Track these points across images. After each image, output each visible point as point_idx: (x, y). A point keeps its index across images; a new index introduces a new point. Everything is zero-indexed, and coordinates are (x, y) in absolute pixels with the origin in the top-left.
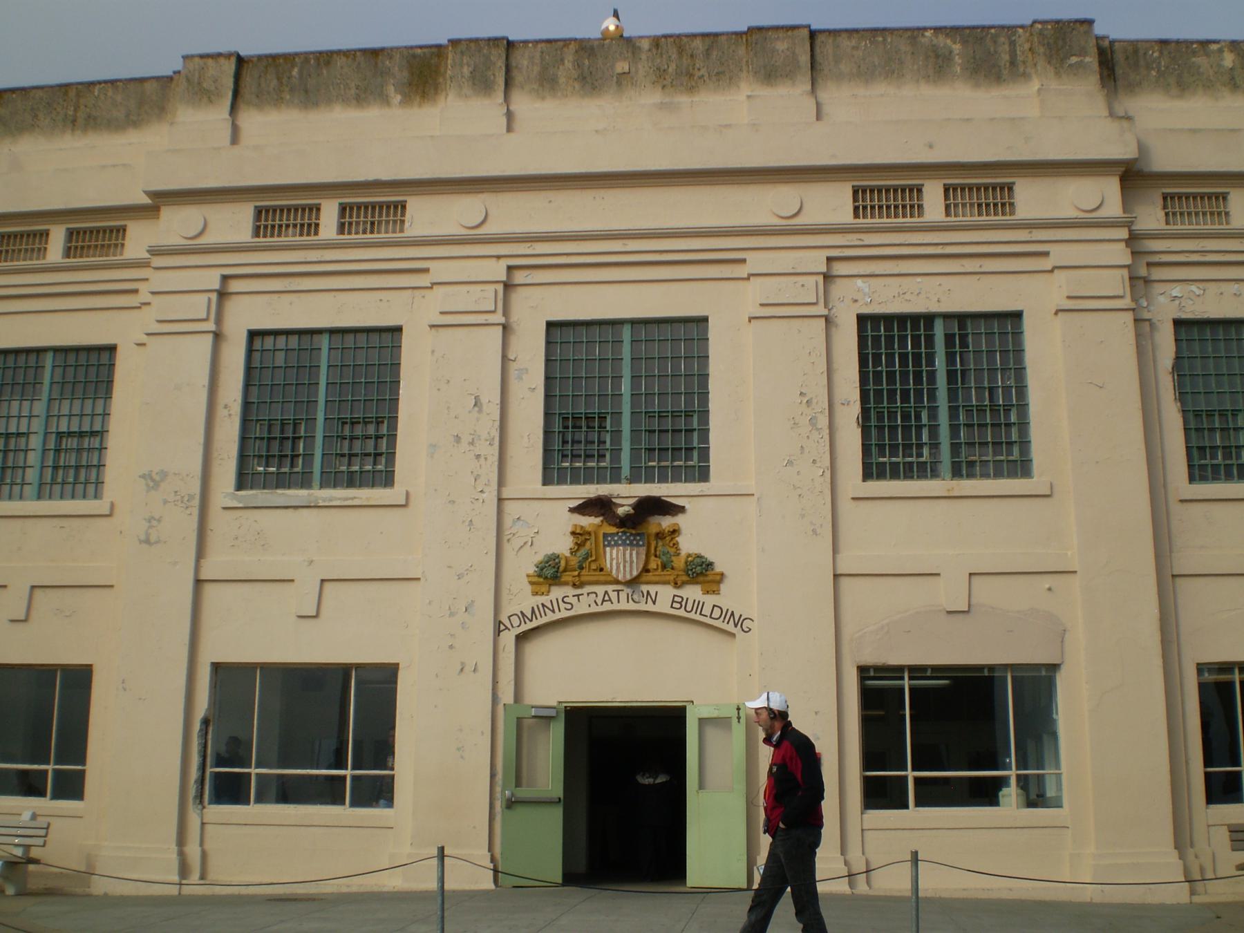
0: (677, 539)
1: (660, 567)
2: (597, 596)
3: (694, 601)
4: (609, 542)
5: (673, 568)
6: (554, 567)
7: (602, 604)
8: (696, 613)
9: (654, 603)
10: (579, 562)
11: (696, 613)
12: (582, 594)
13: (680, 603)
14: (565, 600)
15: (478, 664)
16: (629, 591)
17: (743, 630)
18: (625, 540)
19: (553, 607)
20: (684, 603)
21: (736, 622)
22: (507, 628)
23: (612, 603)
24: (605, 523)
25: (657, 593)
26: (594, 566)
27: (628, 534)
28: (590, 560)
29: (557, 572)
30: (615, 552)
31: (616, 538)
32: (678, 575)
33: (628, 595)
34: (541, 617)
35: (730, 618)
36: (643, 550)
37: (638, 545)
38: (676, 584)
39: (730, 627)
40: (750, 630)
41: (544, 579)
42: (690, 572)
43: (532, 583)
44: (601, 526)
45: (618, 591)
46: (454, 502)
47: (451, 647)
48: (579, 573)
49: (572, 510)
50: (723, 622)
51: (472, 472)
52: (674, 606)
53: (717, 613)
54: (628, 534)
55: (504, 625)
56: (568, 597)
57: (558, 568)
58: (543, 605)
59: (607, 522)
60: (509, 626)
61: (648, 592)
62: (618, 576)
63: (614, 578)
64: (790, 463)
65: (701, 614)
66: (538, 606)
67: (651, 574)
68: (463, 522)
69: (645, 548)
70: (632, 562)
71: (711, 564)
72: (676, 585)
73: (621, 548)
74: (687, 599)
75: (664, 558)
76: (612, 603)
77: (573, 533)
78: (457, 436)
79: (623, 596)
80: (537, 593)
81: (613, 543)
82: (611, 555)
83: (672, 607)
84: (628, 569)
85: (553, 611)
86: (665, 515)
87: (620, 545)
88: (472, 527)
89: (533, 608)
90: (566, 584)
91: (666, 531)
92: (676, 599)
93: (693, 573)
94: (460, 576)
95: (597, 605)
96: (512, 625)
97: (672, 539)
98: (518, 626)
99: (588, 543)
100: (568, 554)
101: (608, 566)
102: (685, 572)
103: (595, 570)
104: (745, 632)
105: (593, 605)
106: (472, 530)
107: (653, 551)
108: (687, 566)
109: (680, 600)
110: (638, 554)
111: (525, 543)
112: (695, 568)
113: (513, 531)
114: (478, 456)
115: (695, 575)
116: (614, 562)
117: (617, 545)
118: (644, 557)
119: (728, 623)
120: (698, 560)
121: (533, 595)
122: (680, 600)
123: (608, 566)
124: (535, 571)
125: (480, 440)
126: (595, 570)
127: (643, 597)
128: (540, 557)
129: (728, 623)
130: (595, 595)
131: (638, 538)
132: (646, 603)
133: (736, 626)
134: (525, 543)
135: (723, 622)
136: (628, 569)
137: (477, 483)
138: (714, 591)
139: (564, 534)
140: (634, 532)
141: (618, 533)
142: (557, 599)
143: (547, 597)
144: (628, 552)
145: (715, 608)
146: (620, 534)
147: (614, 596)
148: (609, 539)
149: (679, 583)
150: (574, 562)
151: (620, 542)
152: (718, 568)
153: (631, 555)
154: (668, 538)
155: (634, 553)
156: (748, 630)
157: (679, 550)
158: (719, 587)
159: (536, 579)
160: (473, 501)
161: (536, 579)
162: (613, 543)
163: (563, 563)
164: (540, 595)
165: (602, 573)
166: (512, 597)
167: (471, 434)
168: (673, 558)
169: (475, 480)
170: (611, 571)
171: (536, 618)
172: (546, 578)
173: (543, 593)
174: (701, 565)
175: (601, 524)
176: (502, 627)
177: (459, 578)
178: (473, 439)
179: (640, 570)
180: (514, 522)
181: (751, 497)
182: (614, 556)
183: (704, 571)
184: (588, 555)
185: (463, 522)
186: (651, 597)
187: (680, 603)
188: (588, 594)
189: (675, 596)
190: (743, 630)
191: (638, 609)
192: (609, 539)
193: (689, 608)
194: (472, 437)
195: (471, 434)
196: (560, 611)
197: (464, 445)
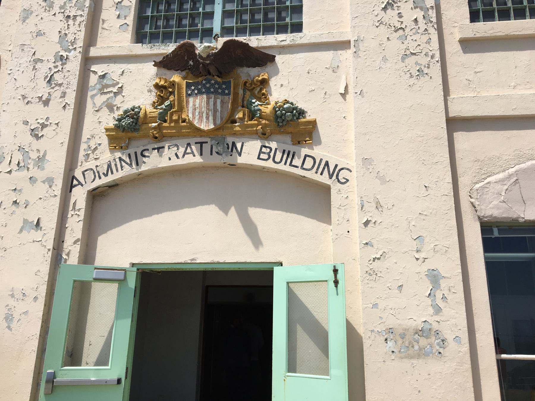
7: (184, 156)
8: (285, 164)
11: (285, 164)
17: (339, 181)
18: (209, 89)
19: (131, 161)
20: (272, 154)
21: (331, 173)
22: (80, 183)
23: (194, 156)
27: (213, 82)
34: (117, 170)
35: (324, 168)
36: (229, 100)
39: (324, 179)
40: (348, 180)
45: (201, 144)
47: (15, 202)
50: (316, 173)
52: (261, 157)
53: (309, 163)
54: (213, 82)
55: (77, 180)
56: (148, 150)
58: (120, 159)
59: (192, 73)
65: (291, 165)
71: (302, 113)
73: (205, 96)
76: (194, 156)
81: (196, 92)
83: (259, 158)
100: (150, 109)
101: (190, 115)
104: (343, 183)
105: (174, 158)
109: (268, 150)
110: (222, 102)
114: (68, 17)
116: (197, 111)
119: (321, 174)
127: (228, 148)
129: (321, 174)
133: (331, 177)
135: (316, 173)
140: (219, 80)
142: (136, 153)
144: (212, 101)
145: (307, 158)
146: (204, 82)
148: (193, 88)
150: (156, 113)
151: (204, 90)
153: (215, 104)
155: (219, 101)
156: (345, 180)
171: (112, 173)
172: (124, 130)
176: (75, 182)
184: (171, 106)
190: (339, 181)
192: (193, 88)
193: (278, 159)
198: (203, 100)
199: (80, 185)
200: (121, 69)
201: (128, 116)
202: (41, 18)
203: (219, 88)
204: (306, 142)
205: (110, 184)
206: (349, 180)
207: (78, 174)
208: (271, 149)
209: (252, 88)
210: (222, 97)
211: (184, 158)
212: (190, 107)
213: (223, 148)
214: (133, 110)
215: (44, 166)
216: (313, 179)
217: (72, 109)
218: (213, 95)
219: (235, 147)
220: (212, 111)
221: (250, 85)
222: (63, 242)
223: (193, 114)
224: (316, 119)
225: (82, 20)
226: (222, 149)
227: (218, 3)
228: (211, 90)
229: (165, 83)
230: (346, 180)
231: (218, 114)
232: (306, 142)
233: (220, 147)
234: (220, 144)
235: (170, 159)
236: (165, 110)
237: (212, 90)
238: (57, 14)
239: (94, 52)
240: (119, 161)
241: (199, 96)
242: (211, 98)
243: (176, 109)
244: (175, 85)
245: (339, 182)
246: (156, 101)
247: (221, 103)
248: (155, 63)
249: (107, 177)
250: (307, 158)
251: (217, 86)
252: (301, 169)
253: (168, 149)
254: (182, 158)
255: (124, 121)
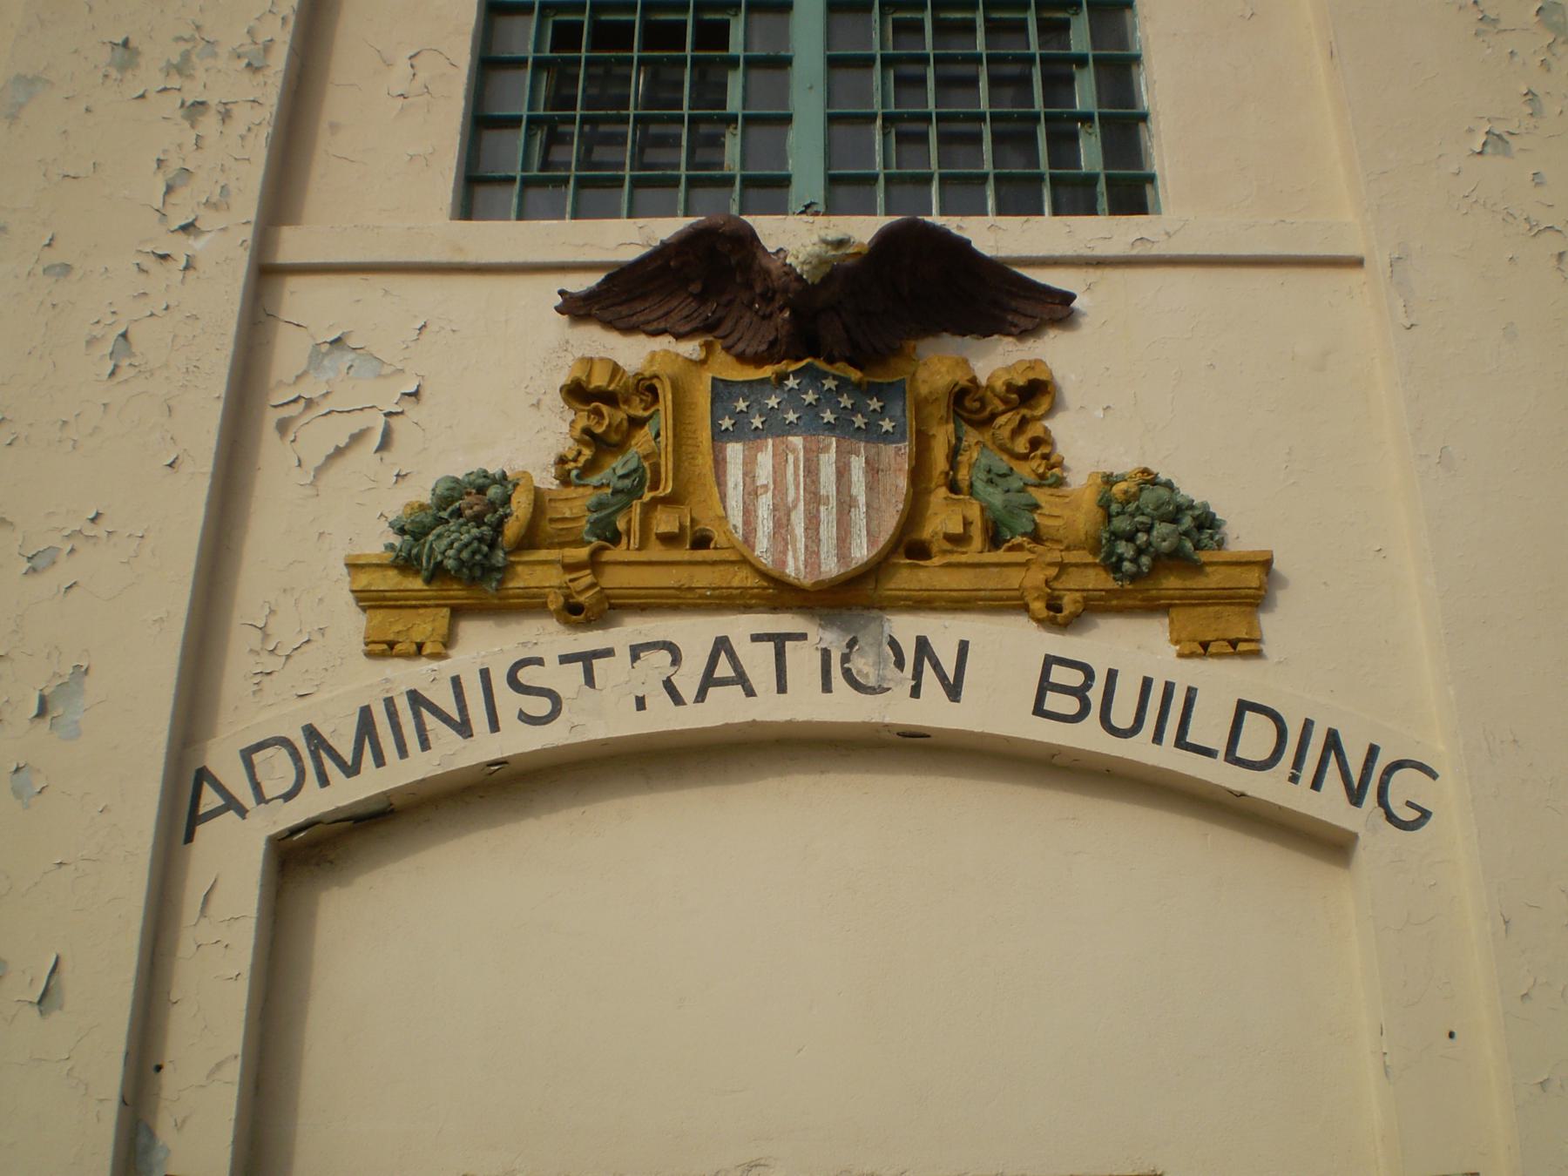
0: (1047, 423)
1: (977, 532)
2: (676, 660)
3: (1147, 684)
4: (741, 418)
5: (1036, 536)
6: (478, 520)
7: (701, 696)
8: (1158, 738)
9: (953, 691)
10: (600, 506)
11: (1158, 738)
12: (608, 653)
13: (1080, 693)
14: (526, 676)
15: (65, 966)
16: (834, 640)
17: (1390, 817)
20: (1096, 695)
21: (1356, 779)
22: (232, 803)
23: (750, 692)
24: (720, 356)
25: (963, 647)
26: (665, 522)
27: (830, 384)
28: (648, 496)
29: (493, 545)
30: (765, 460)
31: (773, 402)
32: (1063, 567)
33: (826, 654)
34: (403, 751)
36: (898, 458)
37: (871, 434)
38: (1054, 606)
40: (1425, 815)
41: (428, 581)
42: (1123, 548)
43: (368, 601)
44: (703, 362)
45: (779, 640)
46: (67, 268)
48: (595, 553)
49: (577, 308)
50: (1294, 779)
51: (160, 162)
53: (1257, 738)
54: (830, 384)
55: (219, 788)
56: (539, 661)
57: (498, 527)
58: (416, 699)
59: (727, 349)
60: (244, 794)
61: (923, 645)
62: (784, 563)
63: (763, 574)
64: (1496, 142)
66: (389, 703)
67: (936, 561)
68: (91, 342)
69: (905, 447)
70: (845, 504)
71: (1207, 522)
72: (1056, 617)
73: (797, 441)
74: (1112, 675)
75: (996, 498)
76: (750, 692)
77: (577, 393)
78: (126, 44)
79: (803, 660)
80: (392, 645)
81: (757, 422)
82: (749, 473)
83: (1039, 710)
84: (828, 532)
85: (463, 728)
86: (986, 333)
87: (791, 429)
88: (125, 363)
89: (366, 713)
90: (532, 605)
91: (999, 385)
92: (1059, 675)
93: (1140, 551)
94: (37, 562)
95: (677, 699)
96: (257, 788)
97: (1024, 422)
98: (288, 796)
99: (646, 433)
100: (546, 480)
101: (736, 517)
102: (1095, 551)
103: (668, 540)
105: (658, 699)
106: (120, 376)
107: (940, 461)
108: (1109, 517)
109: (1075, 678)
110: (872, 469)
111: (357, 438)
112: (1148, 530)
113: (308, 390)
114: (195, 109)
115: (1145, 560)
116: (765, 503)
117: (776, 428)
118: (903, 482)
119: (1316, 784)
120: (1149, 497)
121: (370, 655)
122: (1075, 678)
123: (736, 517)
124: (390, 547)
125: (215, 55)
126: (668, 540)
127: (900, 664)
128: (421, 492)
129: (1316, 784)
130: (665, 657)
131: (875, 404)
132: (915, 692)
133: (1356, 797)
134: (357, 438)
135: (1294, 779)
136: (828, 532)
137: (172, 199)
138: (1233, 643)
139: (537, 405)
140: (855, 375)
141: (781, 378)
142: (485, 674)
143: (435, 665)
144: (828, 464)
145: (1249, 715)
146: (792, 383)
147: (760, 662)
148: (742, 405)
149: (1069, 603)
150: (576, 505)
151: (792, 417)
152: (1242, 536)
153: (842, 473)
154: (1006, 422)
155: (857, 464)
156: (1417, 814)
157: (1060, 464)
158: (1253, 625)
159: (391, 581)
160: (150, 263)
161: (391, 581)
162: (757, 422)
163: (520, 506)
164: (406, 656)
165: (701, 555)
166: (270, 663)
167: (180, 39)
168: (1040, 496)
169: (169, 189)
170: (749, 540)
171: (380, 760)
172: (437, 573)
173: (420, 646)
174: (1174, 519)
175: (703, 355)
176: (210, 800)
177: (34, 570)
178: (186, 56)
179: (884, 538)
180: (316, 357)
181: (1352, 277)
182: (764, 473)
183: (1189, 545)
185: (91, 342)
186: (936, 666)
187: (1080, 693)
188: (636, 652)
189: (1050, 661)
190: (1390, 817)
191: (876, 718)
192: (742, 405)
193: (1123, 715)
194: (184, 46)
195: (180, 39)
196: (494, 725)
197: (149, 75)
198: (791, 458)
199: (232, 812)
200: (415, 317)
201: (458, 513)
202: (88, 110)
203: (855, 409)
204: (1235, 648)
205: (360, 811)
206: (1430, 813)
207: (222, 759)
208: (1089, 673)
209: (987, 413)
210: (870, 445)
211: (703, 701)
212: (730, 484)
213: (880, 662)
214: (481, 490)
215: (77, 722)
216: (1280, 807)
217: (204, 474)
218: (834, 439)
219: (930, 660)
220: (833, 502)
221: (977, 405)
222: (159, 1068)
223: (749, 513)
224: (1272, 556)
225: (257, 122)
226: (873, 665)
227: (808, 85)
228: (823, 418)
229: (611, 381)
230: (1420, 814)
231: (859, 516)
232: (1235, 648)
233: (862, 657)
234: (861, 642)
235: (641, 703)
236: (615, 492)
237: (828, 416)
238: (152, 95)
239: (293, 246)
240: (412, 709)
241: (770, 441)
242: (826, 449)
243: (664, 490)
244: (660, 391)
245: (1391, 822)
246: (570, 457)
247: (866, 472)
248: (565, 301)
249: (354, 778)
250: (1249, 715)
251: (846, 401)
252: (1226, 760)
253: (629, 658)
254: (696, 701)
255: (439, 536)
